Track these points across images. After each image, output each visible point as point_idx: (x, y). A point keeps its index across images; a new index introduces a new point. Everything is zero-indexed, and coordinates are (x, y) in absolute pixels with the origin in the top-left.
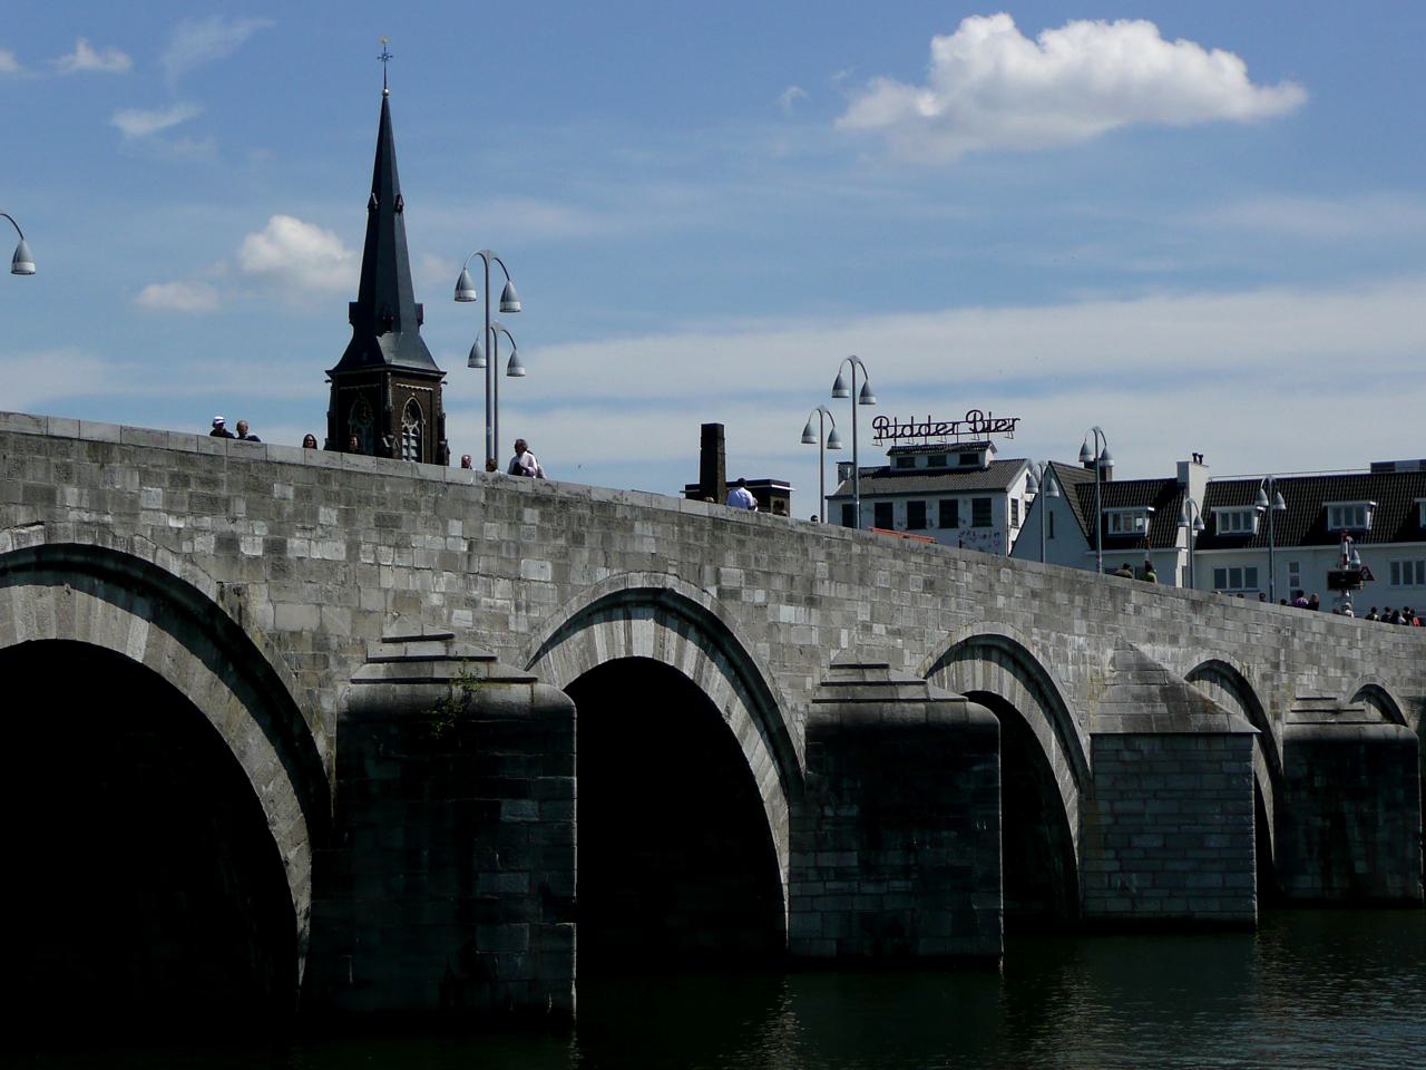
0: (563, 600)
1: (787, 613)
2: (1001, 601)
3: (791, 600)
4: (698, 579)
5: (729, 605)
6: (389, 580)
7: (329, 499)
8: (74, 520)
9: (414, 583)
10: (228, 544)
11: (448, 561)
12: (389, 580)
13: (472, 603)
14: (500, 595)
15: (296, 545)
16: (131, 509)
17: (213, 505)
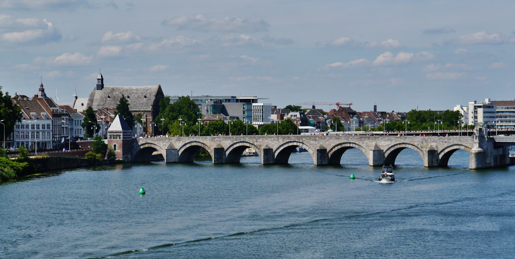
0: (283, 142)
1: (312, 142)
2: (350, 139)
3: (312, 141)
4: (299, 140)
5: (304, 141)
6: (266, 142)
7: (261, 138)
8: (242, 140)
9: (268, 142)
10: (253, 141)
11: (271, 140)
12: (266, 142)
13: (274, 143)
14: (277, 142)
15: (258, 140)
16: (245, 139)
17: (250, 139)
